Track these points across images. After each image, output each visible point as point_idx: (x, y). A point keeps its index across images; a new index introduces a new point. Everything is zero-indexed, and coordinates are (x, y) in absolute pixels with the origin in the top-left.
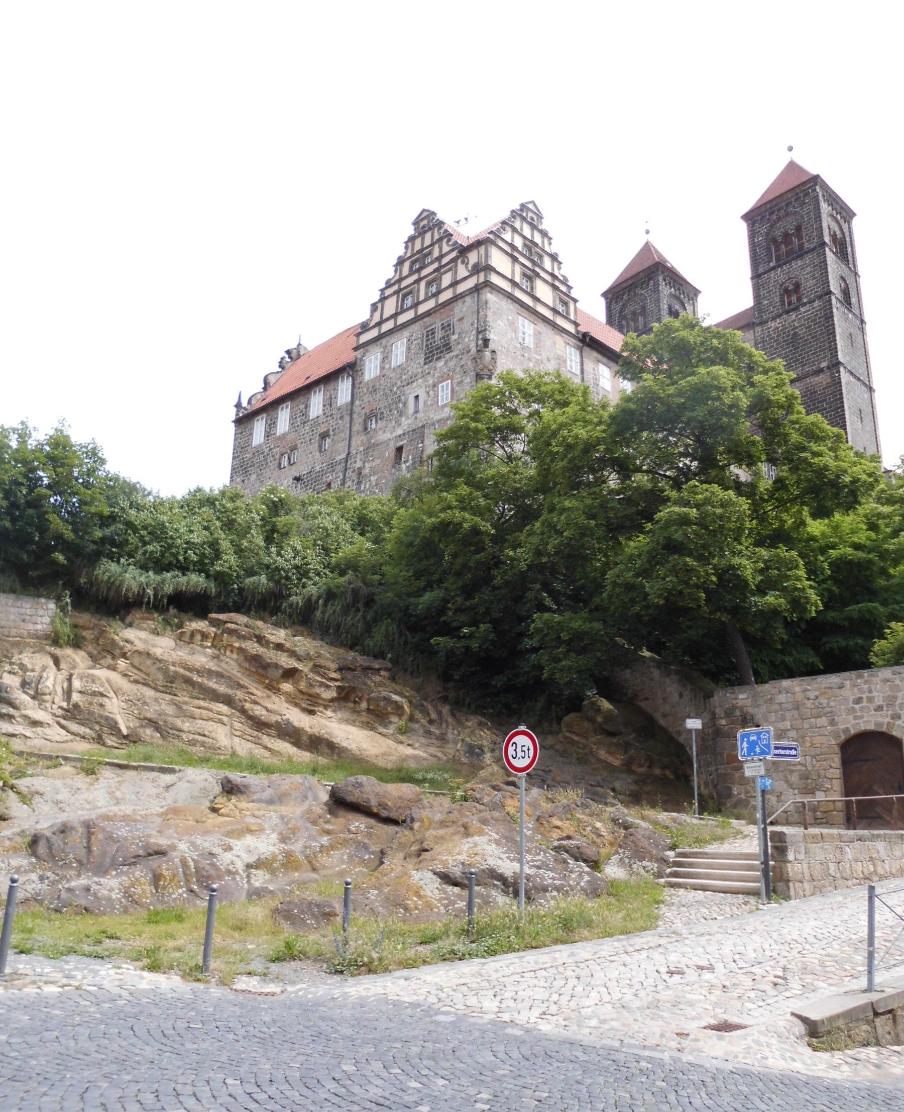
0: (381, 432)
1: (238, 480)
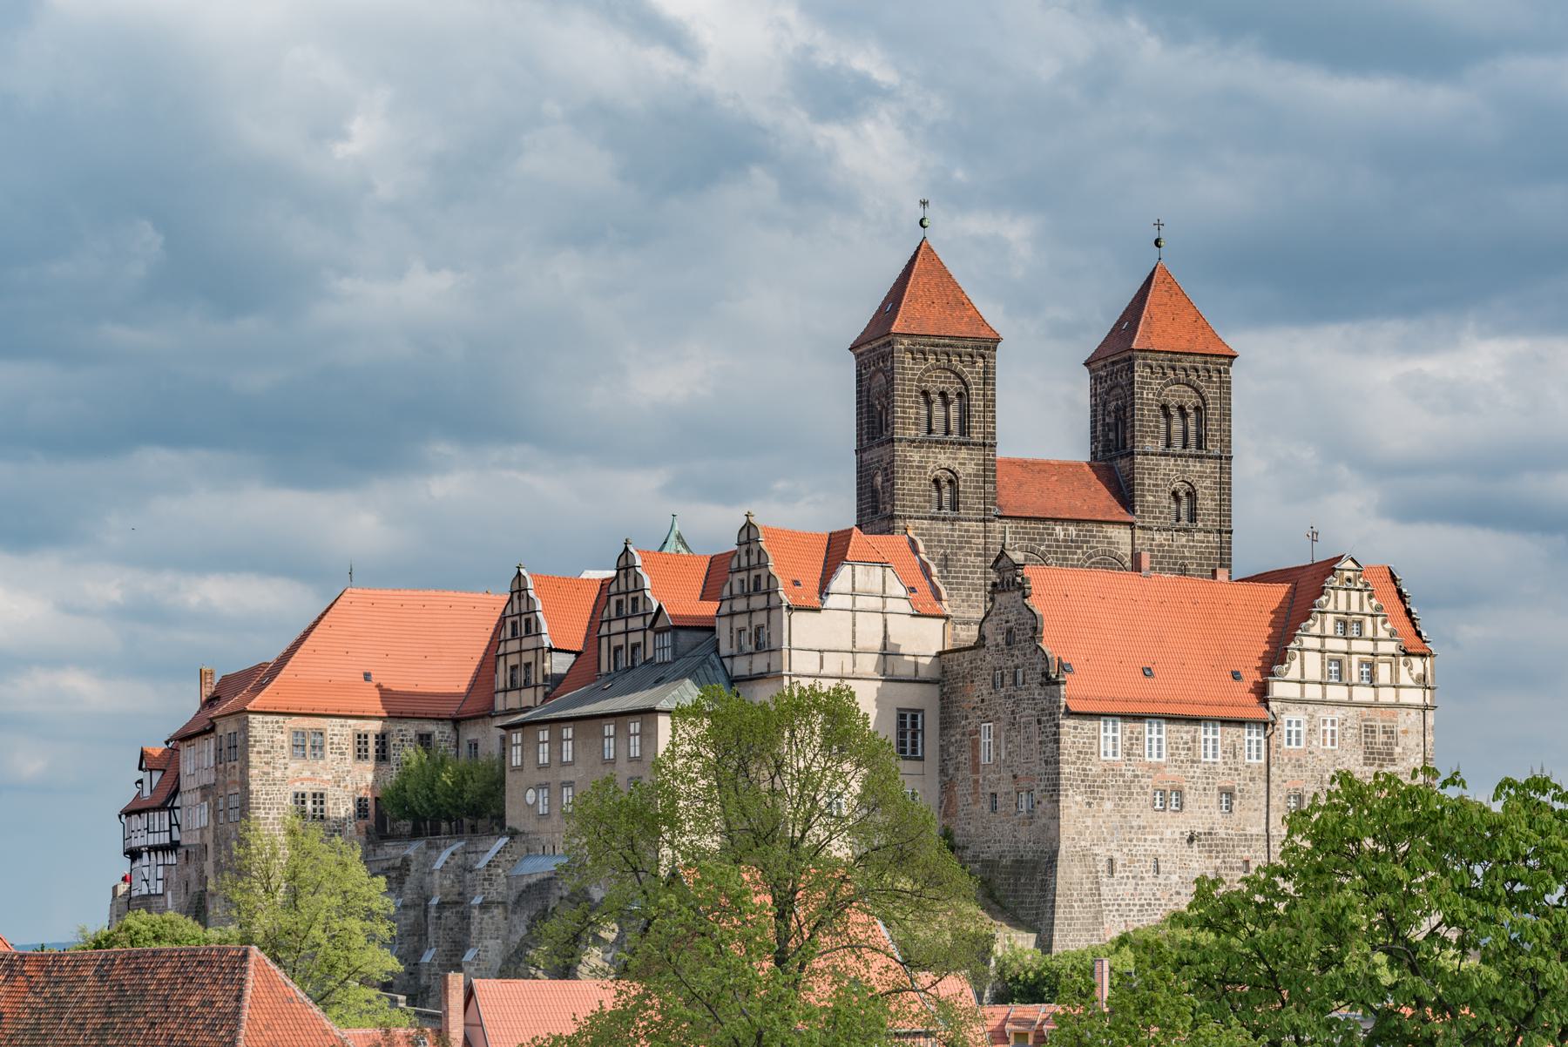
1: (1078, 798)
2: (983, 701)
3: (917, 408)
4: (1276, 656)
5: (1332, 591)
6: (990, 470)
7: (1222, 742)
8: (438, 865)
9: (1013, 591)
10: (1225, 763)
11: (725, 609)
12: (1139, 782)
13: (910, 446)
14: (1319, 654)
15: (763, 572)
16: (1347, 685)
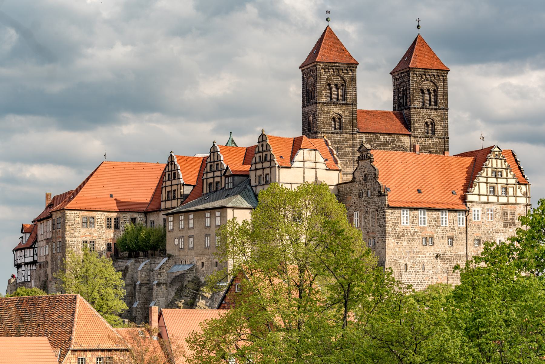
1: (393, 241)
2: (355, 203)
3: (326, 90)
4: (469, 185)
5: (490, 160)
6: (355, 114)
7: (449, 218)
8: (140, 269)
9: (367, 160)
10: (450, 227)
11: (253, 168)
12: (417, 234)
13: (323, 105)
14: (486, 184)
15: (268, 153)
16: (497, 196)
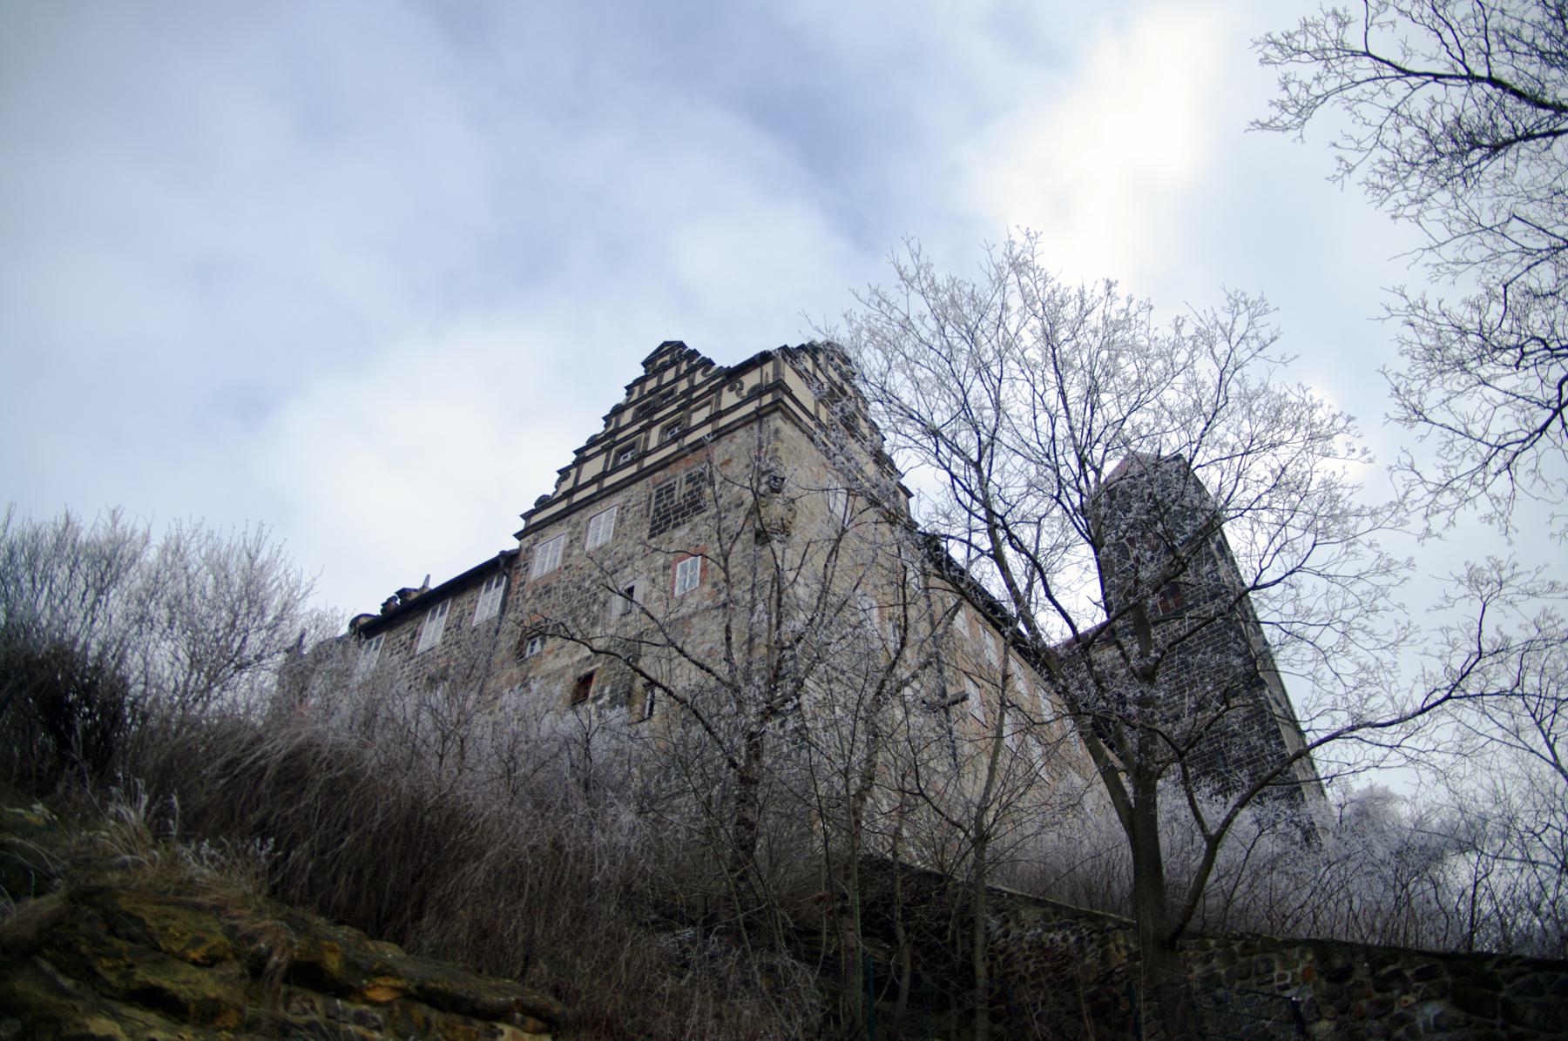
0: (550, 657)
